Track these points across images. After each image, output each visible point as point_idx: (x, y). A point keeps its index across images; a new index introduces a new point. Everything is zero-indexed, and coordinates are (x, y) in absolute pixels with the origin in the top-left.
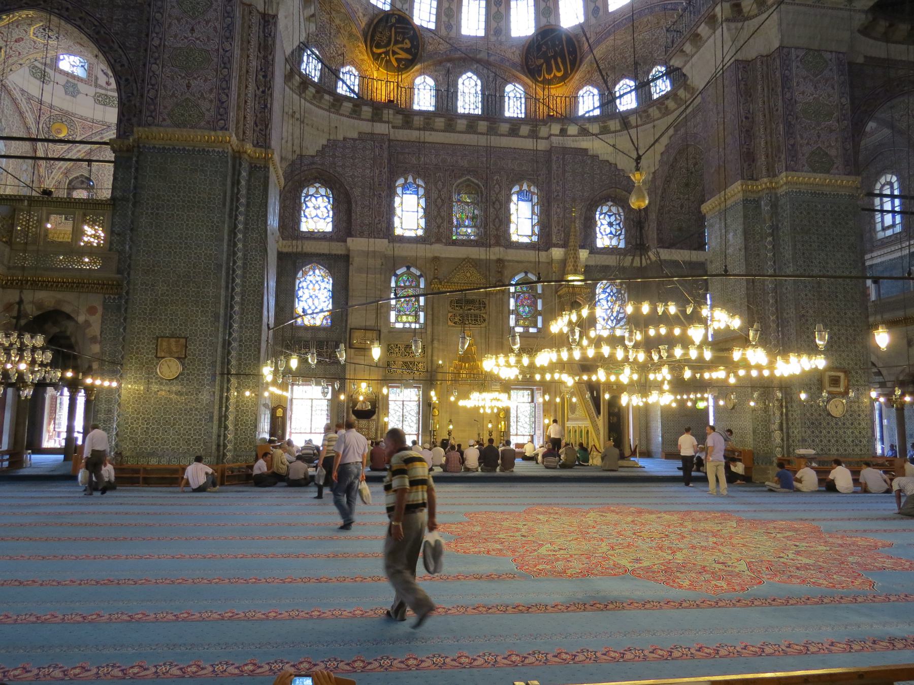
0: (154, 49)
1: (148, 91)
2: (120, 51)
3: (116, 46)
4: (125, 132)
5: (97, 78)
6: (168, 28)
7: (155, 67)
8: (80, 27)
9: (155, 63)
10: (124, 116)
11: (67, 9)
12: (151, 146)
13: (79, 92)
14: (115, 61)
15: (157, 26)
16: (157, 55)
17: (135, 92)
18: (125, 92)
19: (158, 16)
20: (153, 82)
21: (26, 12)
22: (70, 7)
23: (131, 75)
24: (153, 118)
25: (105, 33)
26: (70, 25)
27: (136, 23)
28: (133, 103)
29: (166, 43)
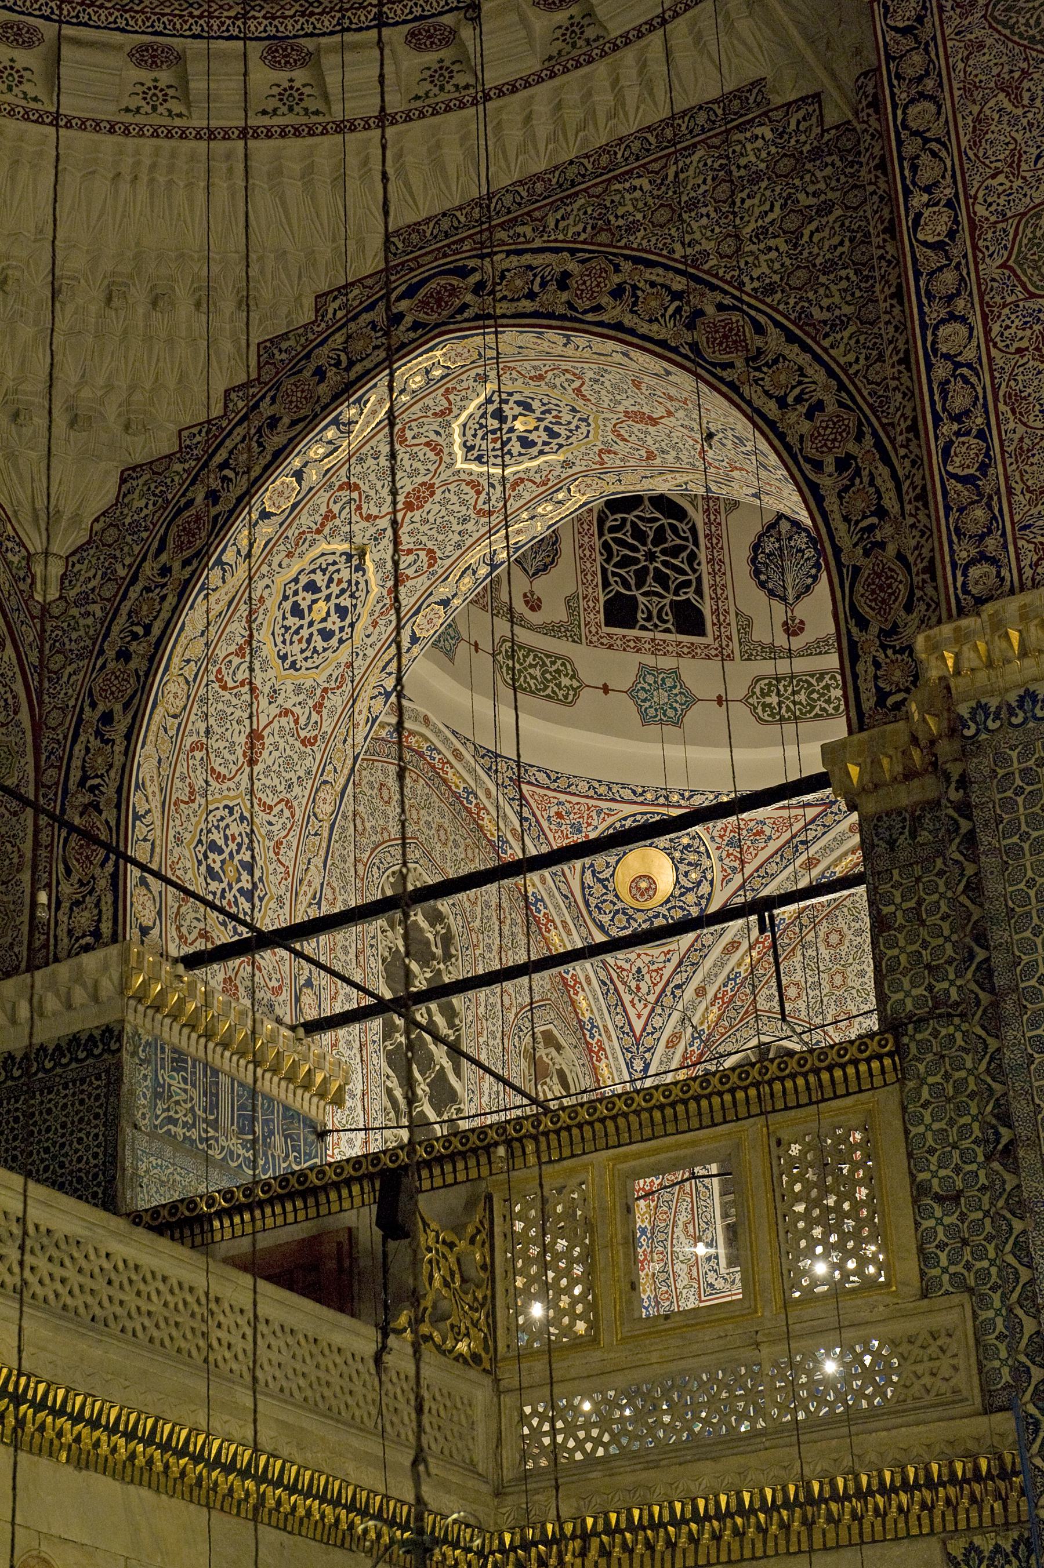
0: (935, 259)
1: (946, 453)
2: (793, 351)
3: (774, 340)
4: (882, 696)
5: (746, 625)
6: (975, 144)
7: (951, 337)
8: (619, 326)
9: (952, 317)
10: (863, 624)
11: (563, 281)
12: (1012, 698)
13: (691, 700)
14: (782, 403)
15: (925, 158)
16: (949, 277)
17: (890, 502)
18: (846, 519)
19: (920, 114)
20: (959, 402)
21: (423, 361)
22: (572, 267)
23: (859, 438)
24: (994, 561)
25: (721, 307)
26: (581, 340)
27: (837, 212)
28: (891, 549)
29: (981, 210)
